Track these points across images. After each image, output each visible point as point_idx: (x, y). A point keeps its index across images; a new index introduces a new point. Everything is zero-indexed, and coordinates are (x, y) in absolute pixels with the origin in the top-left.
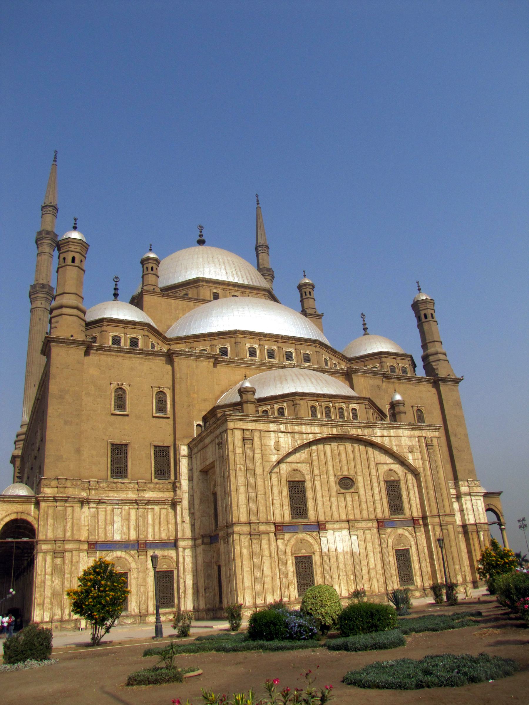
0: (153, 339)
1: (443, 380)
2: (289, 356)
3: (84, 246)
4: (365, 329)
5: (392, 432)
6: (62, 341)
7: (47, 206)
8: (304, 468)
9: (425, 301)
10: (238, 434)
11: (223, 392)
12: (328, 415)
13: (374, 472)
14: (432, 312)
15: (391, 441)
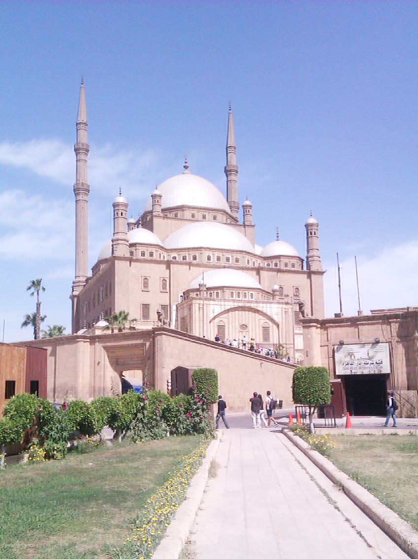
0: (160, 251)
1: (315, 273)
2: (228, 259)
3: (126, 205)
4: (278, 237)
5: (268, 305)
6: (119, 258)
7: (81, 123)
8: (226, 321)
9: (312, 225)
10: (197, 306)
11: (193, 280)
12: (239, 297)
13: (257, 323)
14: (316, 231)
15: (266, 310)
